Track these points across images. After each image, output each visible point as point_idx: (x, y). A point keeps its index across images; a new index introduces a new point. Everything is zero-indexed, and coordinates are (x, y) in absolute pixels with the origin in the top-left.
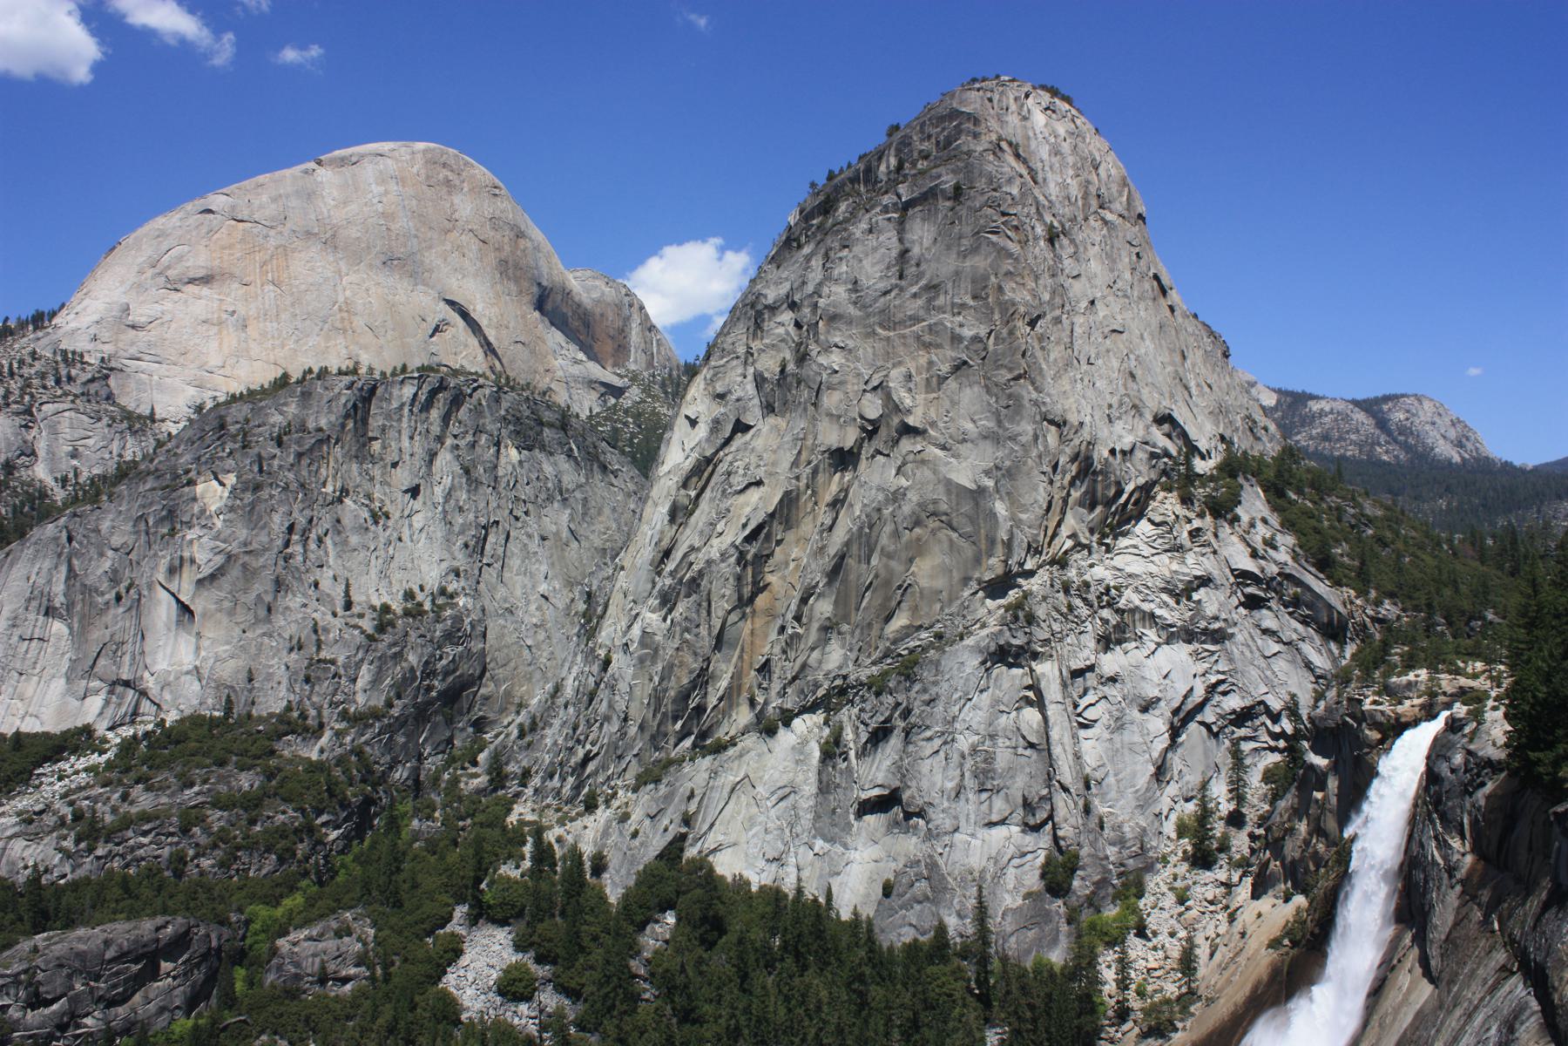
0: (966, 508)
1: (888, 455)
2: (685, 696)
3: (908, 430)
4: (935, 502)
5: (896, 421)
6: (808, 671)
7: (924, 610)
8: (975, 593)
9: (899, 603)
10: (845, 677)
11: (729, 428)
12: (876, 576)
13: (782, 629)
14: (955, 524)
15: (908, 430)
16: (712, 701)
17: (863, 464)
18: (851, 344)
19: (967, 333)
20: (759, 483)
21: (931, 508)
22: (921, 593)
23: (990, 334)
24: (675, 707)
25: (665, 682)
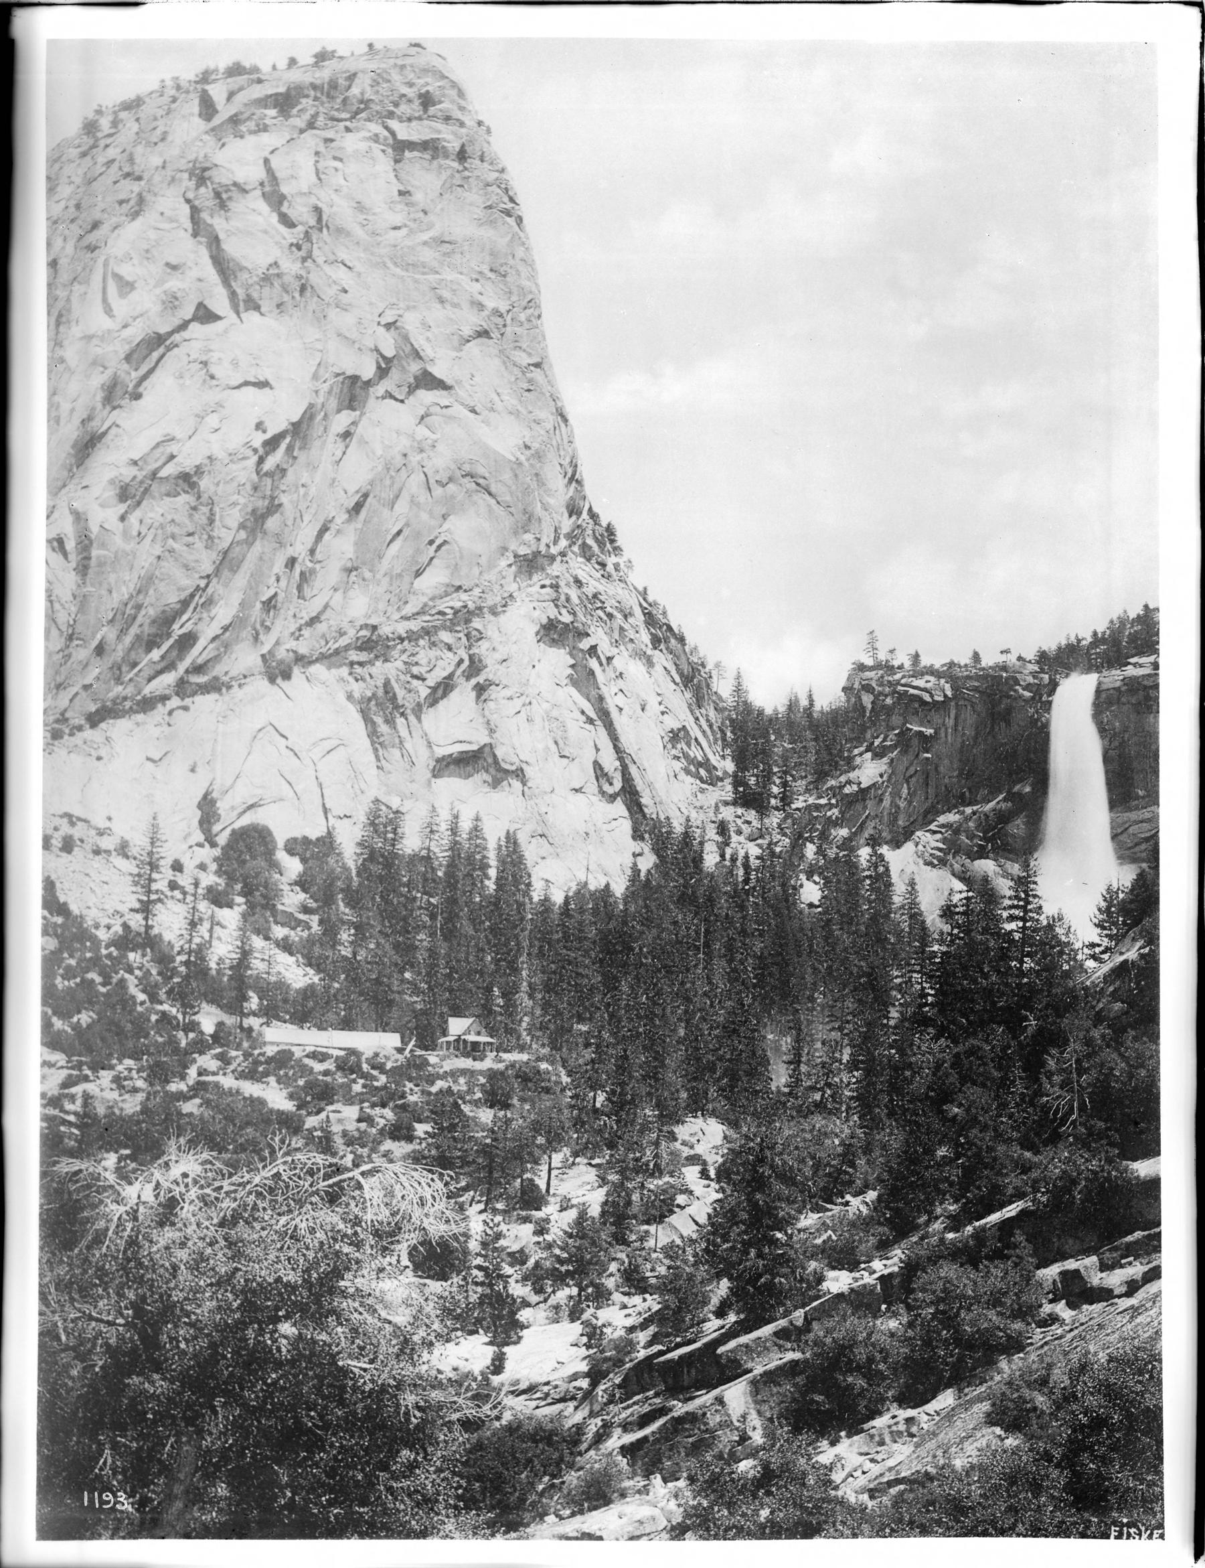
0: (507, 476)
1: (402, 401)
2: (166, 620)
3: (427, 381)
4: (471, 462)
5: (415, 367)
6: (329, 611)
7: (464, 571)
8: (510, 565)
9: (432, 559)
10: (375, 628)
11: (188, 312)
12: (407, 525)
13: (291, 562)
14: (493, 489)
15: (427, 381)
16: (208, 631)
17: (372, 402)
18: (358, 267)
19: (490, 304)
20: (263, 384)
21: (467, 468)
22: (460, 551)
23: (508, 311)
24: (153, 630)
25: (141, 597)
